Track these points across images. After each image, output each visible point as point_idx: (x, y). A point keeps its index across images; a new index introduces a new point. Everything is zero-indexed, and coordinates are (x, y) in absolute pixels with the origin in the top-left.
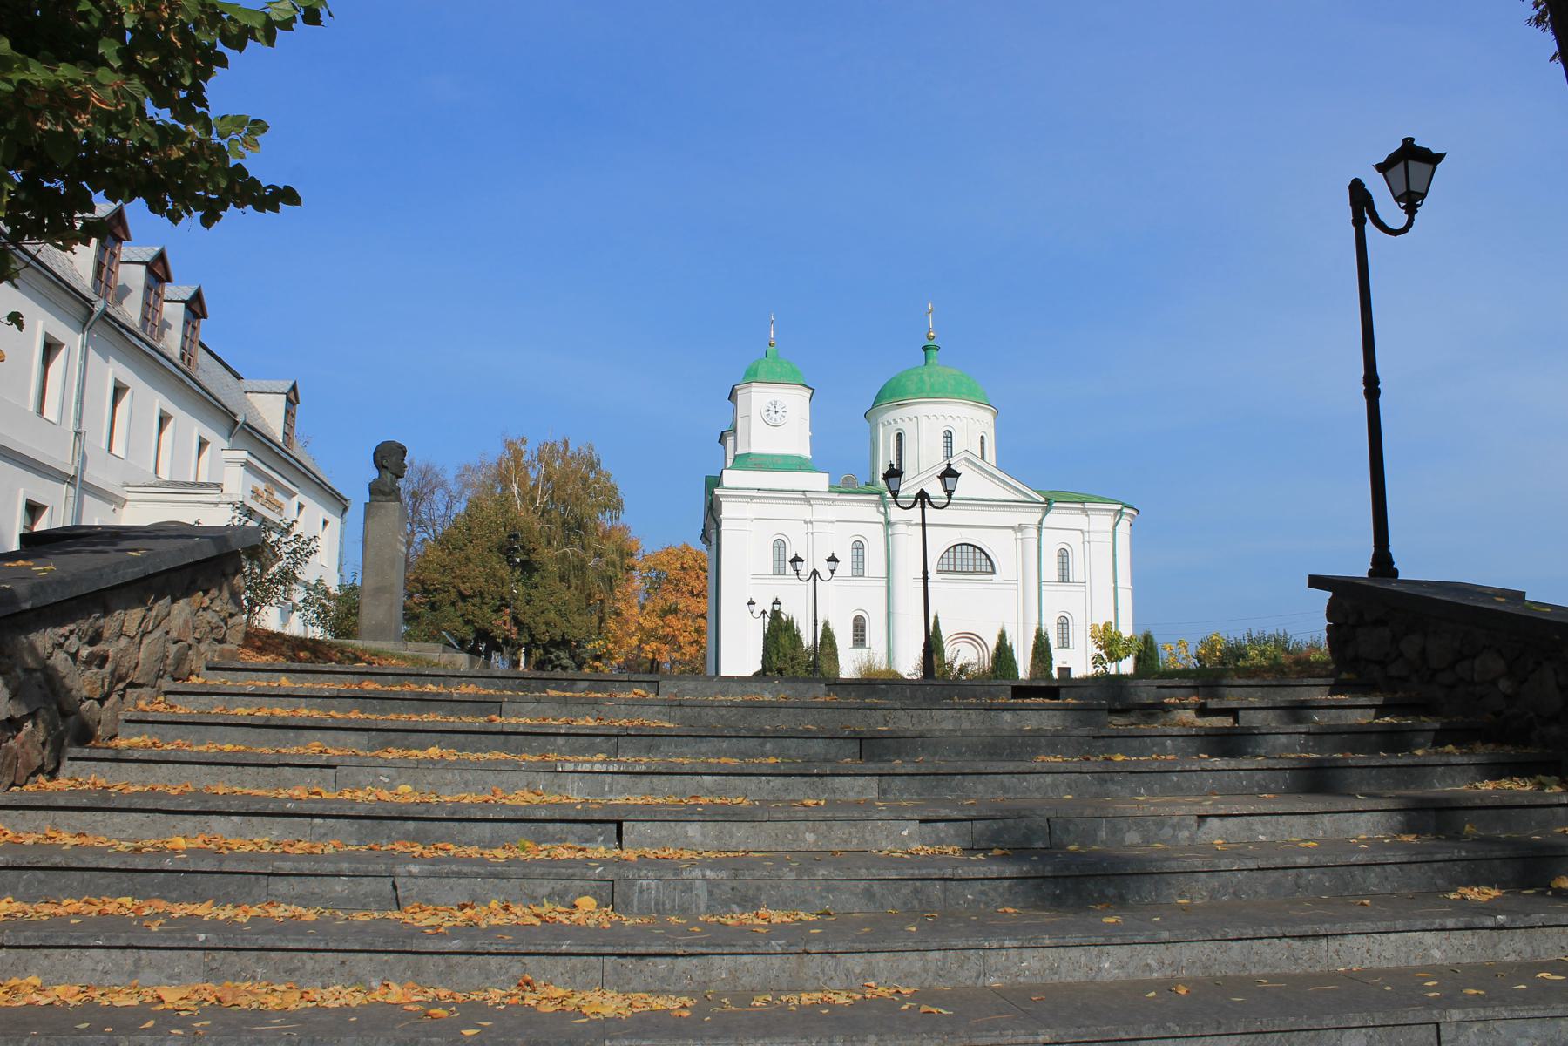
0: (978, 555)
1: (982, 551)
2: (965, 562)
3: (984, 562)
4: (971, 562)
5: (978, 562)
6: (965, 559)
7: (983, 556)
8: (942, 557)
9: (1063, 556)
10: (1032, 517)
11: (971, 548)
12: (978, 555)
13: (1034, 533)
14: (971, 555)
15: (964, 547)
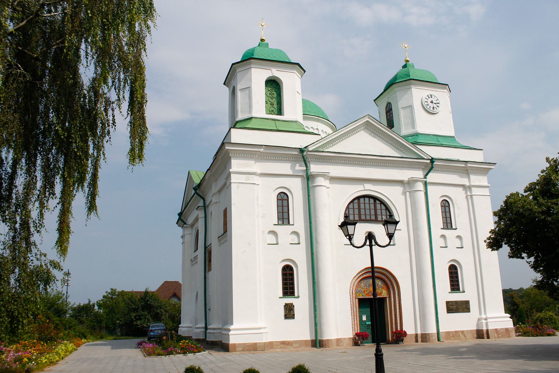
0: (378, 206)
1: (382, 202)
2: (368, 212)
3: (384, 212)
4: (373, 212)
5: (379, 212)
6: (367, 206)
7: (383, 207)
8: (348, 207)
9: (445, 207)
10: (419, 174)
11: (372, 201)
12: (378, 206)
13: (420, 186)
14: (372, 206)
15: (367, 199)
